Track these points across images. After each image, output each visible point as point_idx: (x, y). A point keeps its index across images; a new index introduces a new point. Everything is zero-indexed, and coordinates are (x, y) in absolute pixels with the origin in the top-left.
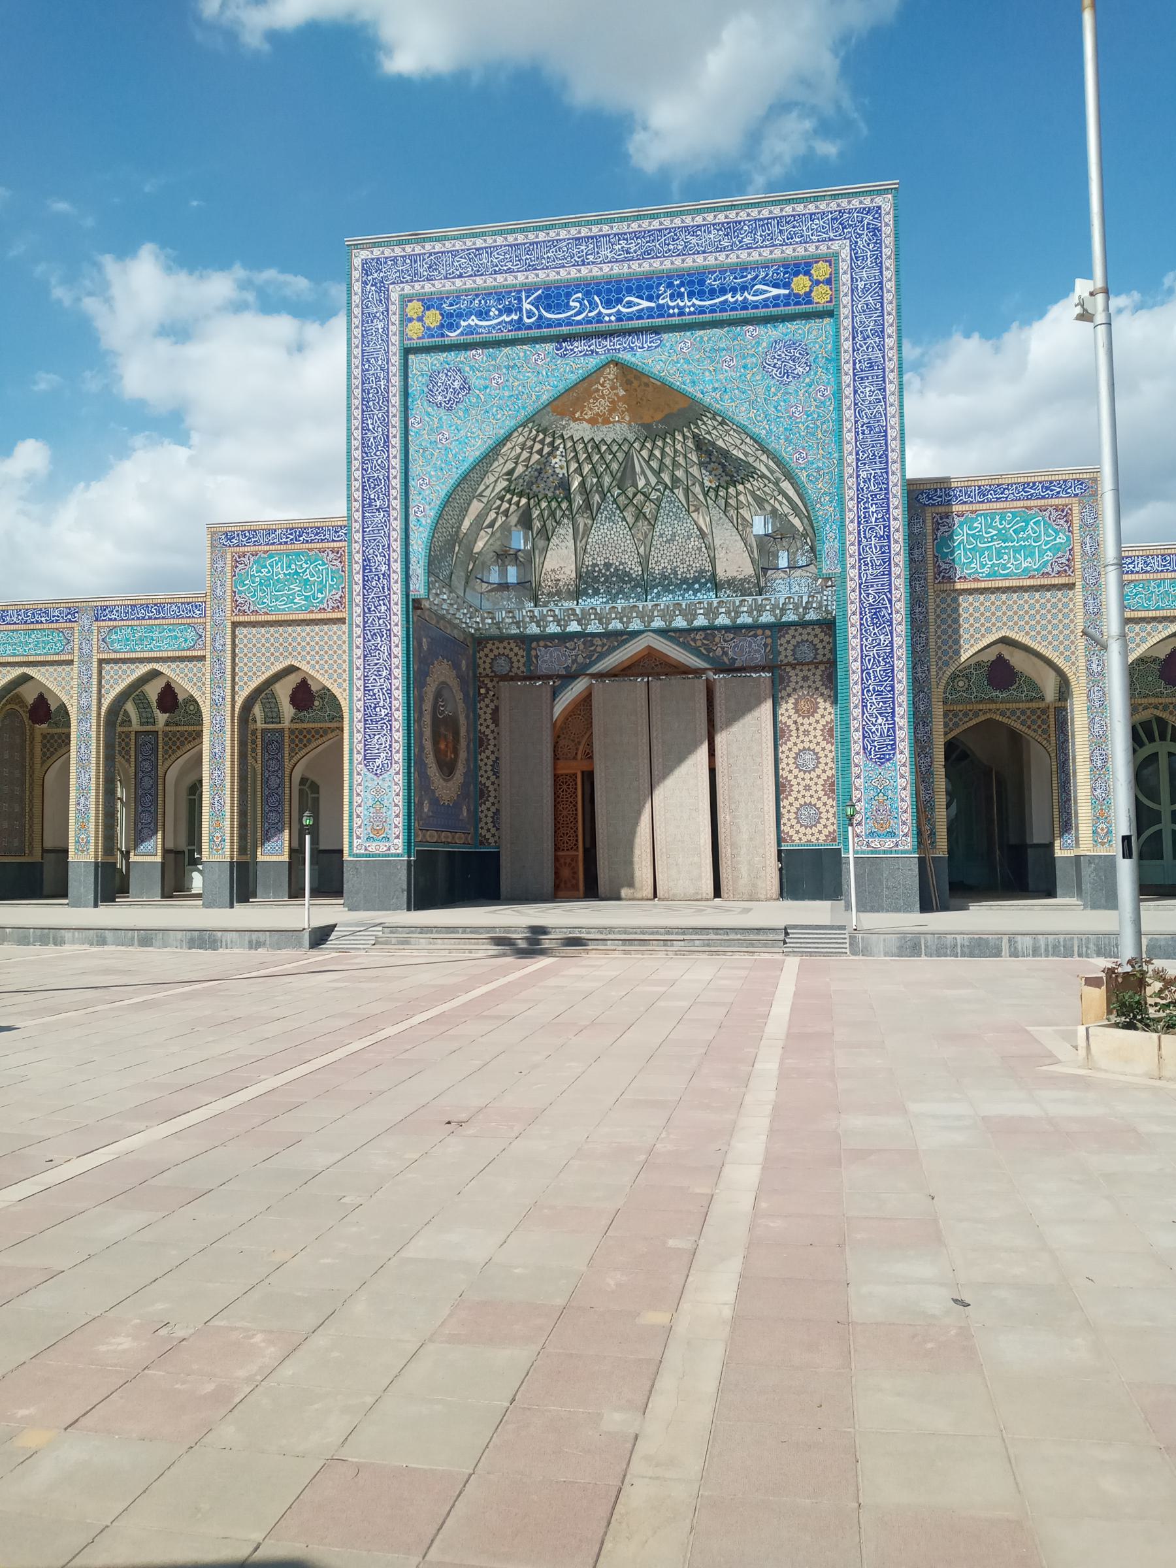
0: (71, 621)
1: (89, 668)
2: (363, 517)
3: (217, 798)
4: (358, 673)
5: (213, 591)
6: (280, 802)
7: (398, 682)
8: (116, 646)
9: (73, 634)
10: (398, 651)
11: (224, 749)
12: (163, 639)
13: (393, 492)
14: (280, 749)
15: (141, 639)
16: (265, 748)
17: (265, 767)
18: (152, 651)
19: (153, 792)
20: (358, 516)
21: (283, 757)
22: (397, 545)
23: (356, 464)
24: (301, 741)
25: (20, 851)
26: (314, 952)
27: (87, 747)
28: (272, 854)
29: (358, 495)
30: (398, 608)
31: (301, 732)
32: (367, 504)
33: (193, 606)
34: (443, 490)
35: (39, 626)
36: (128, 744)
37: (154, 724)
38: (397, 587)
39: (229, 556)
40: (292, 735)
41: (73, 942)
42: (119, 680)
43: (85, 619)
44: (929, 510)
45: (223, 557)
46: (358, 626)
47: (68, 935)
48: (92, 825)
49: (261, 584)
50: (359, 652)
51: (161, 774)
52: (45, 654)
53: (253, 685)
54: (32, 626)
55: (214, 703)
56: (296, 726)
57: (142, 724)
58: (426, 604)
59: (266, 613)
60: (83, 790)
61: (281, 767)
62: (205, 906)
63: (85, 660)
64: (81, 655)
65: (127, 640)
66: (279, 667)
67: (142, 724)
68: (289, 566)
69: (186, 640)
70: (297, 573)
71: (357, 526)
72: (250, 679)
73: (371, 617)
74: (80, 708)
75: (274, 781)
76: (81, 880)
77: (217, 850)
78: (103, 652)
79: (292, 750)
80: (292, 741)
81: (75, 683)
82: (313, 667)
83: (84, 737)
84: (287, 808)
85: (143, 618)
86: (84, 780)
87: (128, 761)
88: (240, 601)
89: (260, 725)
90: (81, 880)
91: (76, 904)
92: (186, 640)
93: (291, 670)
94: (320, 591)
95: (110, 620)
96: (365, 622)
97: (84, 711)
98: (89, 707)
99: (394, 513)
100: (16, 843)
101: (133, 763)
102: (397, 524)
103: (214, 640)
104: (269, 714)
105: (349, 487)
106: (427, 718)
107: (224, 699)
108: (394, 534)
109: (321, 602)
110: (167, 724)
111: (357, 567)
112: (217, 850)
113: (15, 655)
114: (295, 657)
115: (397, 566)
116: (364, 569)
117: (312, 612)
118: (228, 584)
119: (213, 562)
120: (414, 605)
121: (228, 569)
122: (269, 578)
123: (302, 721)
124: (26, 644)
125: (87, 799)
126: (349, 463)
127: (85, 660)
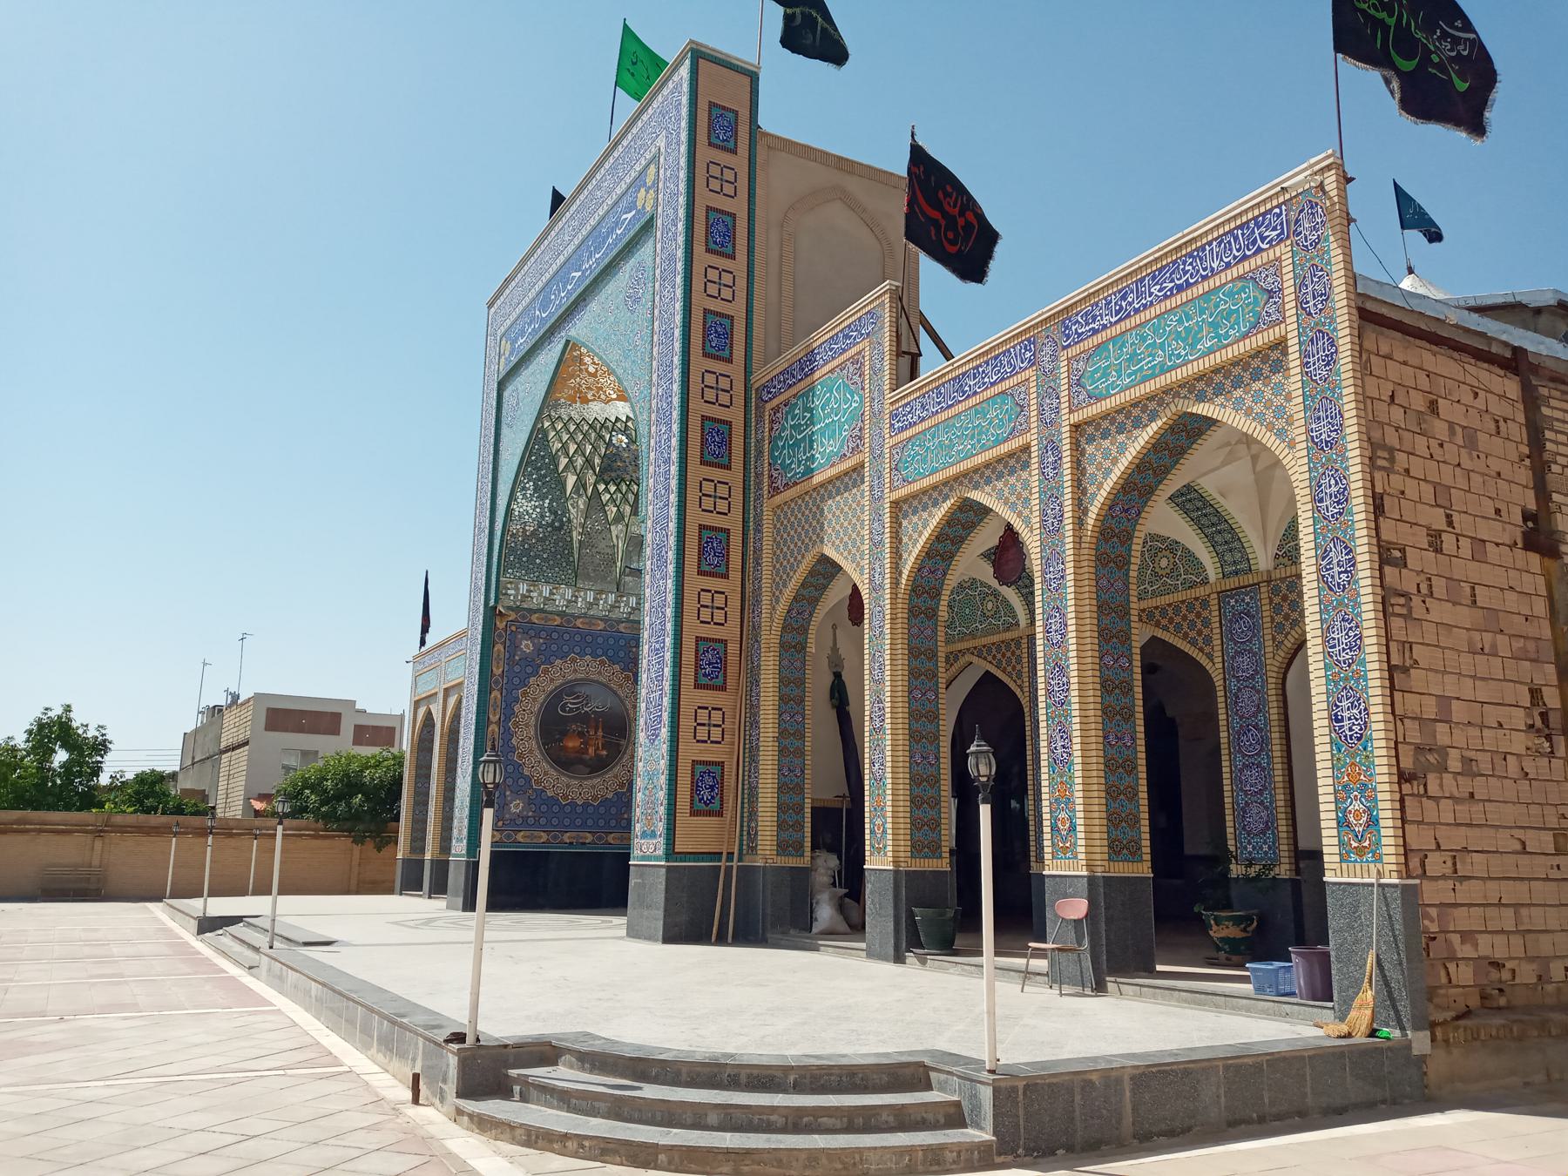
44: (769, 406)
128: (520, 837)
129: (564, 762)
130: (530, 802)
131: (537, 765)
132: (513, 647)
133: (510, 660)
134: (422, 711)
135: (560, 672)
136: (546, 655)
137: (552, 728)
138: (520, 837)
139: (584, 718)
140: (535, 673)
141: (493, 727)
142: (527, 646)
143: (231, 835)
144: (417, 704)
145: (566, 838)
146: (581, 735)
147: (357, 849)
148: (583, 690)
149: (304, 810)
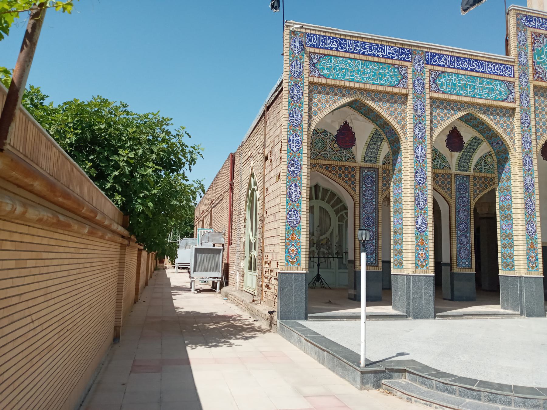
0: (404, 60)
3: (530, 224)
8: (445, 88)
9: (407, 71)
11: (533, 185)
12: (483, 89)
14: (467, 190)
15: (465, 86)
16: (457, 189)
18: (474, 97)
19: (374, 215)
21: (470, 196)
27: (423, 172)
28: (464, 267)
31: (481, 179)
35: (377, 59)
37: (375, 162)
39: (529, 35)
45: (525, 33)
52: (382, 85)
54: (370, 58)
56: (477, 174)
57: (365, 161)
63: (419, 96)
64: (415, 91)
65: (454, 85)
67: (365, 161)
69: (501, 93)
77: (533, 268)
78: (434, 91)
79: (475, 191)
85: (466, 69)
87: (355, 191)
88: (539, 70)
92: (501, 93)
95: (440, 65)
101: (358, 191)
103: (521, 97)
104: (462, 164)
107: (530, 144)
112: (533, 268)
113: (353, 81)
121: (529, 44)
123: (481, 172)
124: (364, 73)
125: (424, 219)
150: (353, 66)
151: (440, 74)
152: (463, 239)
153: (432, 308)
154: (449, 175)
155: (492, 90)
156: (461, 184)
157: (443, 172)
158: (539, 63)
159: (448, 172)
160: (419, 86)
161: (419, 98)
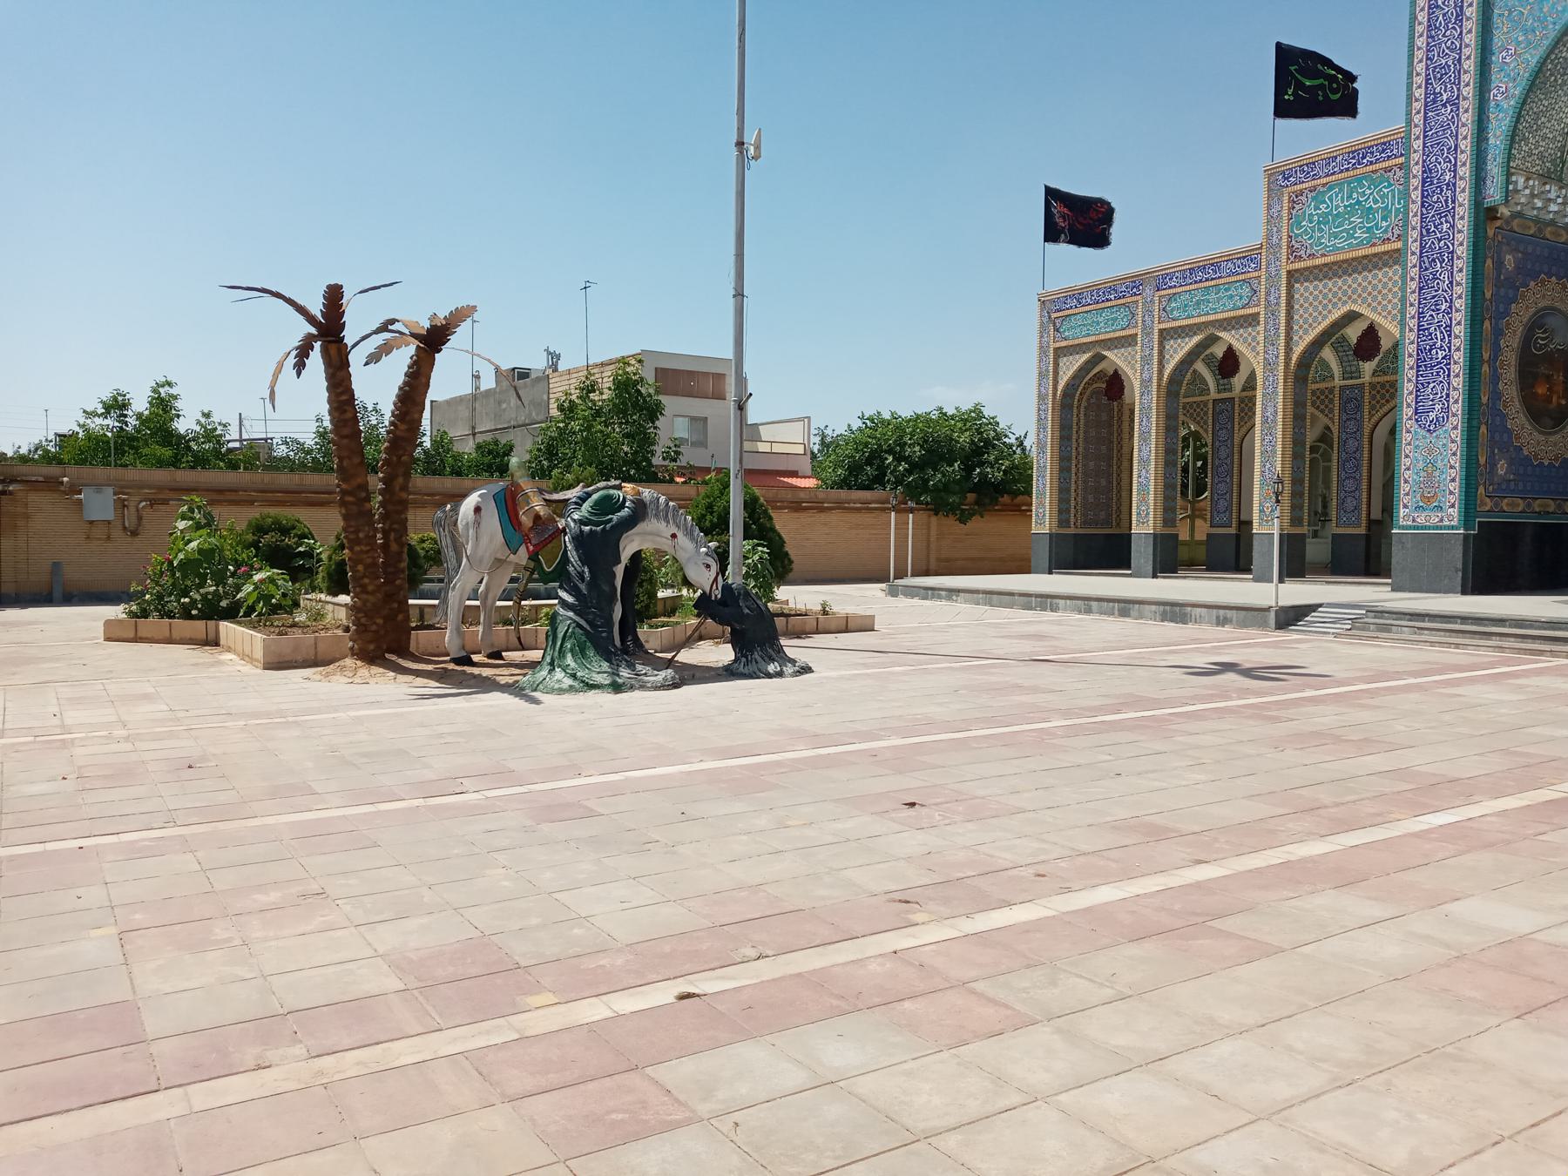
1: (1151, 341)
2: (1425, 118)
4: (1412, 311)
5: (1269, 237)
6: (1358, 467)
7: (1460, 316)
10: (1462, 277)
12: (1219, 299)
13: (1465, 78)
14: (1359, 408)
15: (1198, 303)
16: (1343, 409)
17: (1342, 427)
20: (1418, 119)
22: (1466, 145)
23: (1419, 54)
24: (1383, 397)
25: (1107, 523)
26: (1281, 636)
28: (1349, 526)
29: (1419, 93)
30: (1464, 224)
32: (1432, 101)
33: (1248, 257)
34: (1533, 58)
36: (1242, 410)
37: (1230, 390)
38: (1464, 198)
40: (1347, 393)
41: (1065, 609)
42: (1179, 350)
43: (1148, 291)
46: (1413, 253)
47: (1061, 602)
48: (1151, 497)
49: (1319, 223)
50: (1413, 285)
51: (1237, 441)
53: (1309, 338)
55: (1267, 363)
57: (1219, 392)
58: (1504, 211)
59: (1323, 255)
60: (1144, 462)
61: (1360, 428)
62: (1256, 580)
63: (1147, 332)
66: (1336, 314)
67: (1219, 392)
68: (1350, 197)
70: (1359, 202)
71: (1416, 131)
72: (1306, 332)
73: (1429, 240)
74: (1142, 381)
75: (1352, 444)
76: (1269, 553)
79: (1373, 408)
80: (1373, 397)
81: (1138, 357)
82: (1374, 310)
83: (1146, 411)
84: (1365, 473)
86: (1145, 454)
89: (1338, 382)
90: (1142, 553)
91: (1264, 578)
93: (1352, 317)
94: (1384, 218)
96: (1422, 247)
97: (1145, 383)
98: (1150, 380)
99: (1464, 104)
100: (1103, 515)
102: (1468, 118)
103: (1268, 294)
105: (1410, 85)
106: (1510, 358)
108: (1463, 131)
109: (1386, 231)
110: (1243, 390)
111: (1415, 182)
114: (1355, 302)
115: (1465, 171)
116: (1424, 182)
117: (1374, 245)
118: (1284, 229)
119: (1269, 208)
120: (1485, 215)
121: (1285, 213)
122: (1327, 214)
123: (1385, 373)
126: (1411, 56)
127: (1147, 332)
128: (1504, 504)
129: (1539, 413)
130: (1511, 463)
131: (1517, 418)
132: (1499, 264)
133: (1498, 284)
134: (1071, 366)
135: (1538, 296)
136: (1527, 272)
137: (1530, 367)
138: (1504, 504)
139: (1549, 358)
140: (1514, 300)
141: (1485, 368)
142: (1509, 260)
143: (822, 510)
144: (1059, 353)
145: (1536, 506)
146: (1548, 378)
147: (934, 519)
148: (1551, 322)
149: (878, 481)
150: (1090, 318)
151: (1171, 298)
152: (1350, 485)
153: (1150, 568)
154: (1331, 390)
155: (1231, 297)
156: (1349, 400)
157: (1322, 385)
158: (1297, 236)
159: (1329, 385)
160: (1148, 322)
161: (1148, 334)
